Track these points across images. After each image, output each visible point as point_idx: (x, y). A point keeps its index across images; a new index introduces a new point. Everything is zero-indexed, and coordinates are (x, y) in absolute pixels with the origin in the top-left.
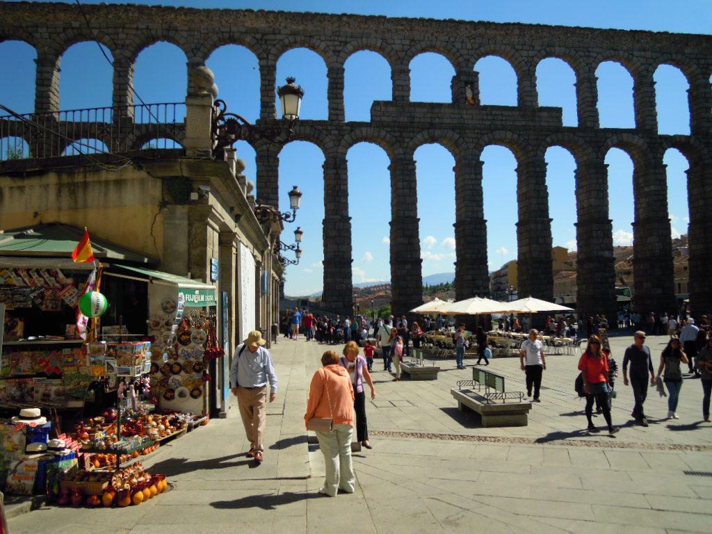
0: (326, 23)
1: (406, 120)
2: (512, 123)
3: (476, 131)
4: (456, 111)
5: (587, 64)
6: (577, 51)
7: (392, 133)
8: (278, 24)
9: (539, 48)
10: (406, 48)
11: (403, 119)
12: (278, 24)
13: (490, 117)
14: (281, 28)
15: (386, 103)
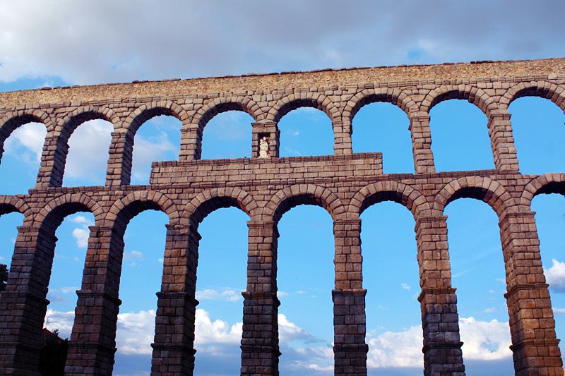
0: (118, 91)
1: (186, 180)
2: (316, 175)
3: (269, 187)
4: (246, 167)
5: (416, 102)
6: (402, 90)
7: (168, 195)
8: (70, 98)
9: (354, 91)
10: (197, 106)
11: (184, 180)
12: (70, 98)
13: (288, 170)
14: (71, 101)
15: (165, 164)
